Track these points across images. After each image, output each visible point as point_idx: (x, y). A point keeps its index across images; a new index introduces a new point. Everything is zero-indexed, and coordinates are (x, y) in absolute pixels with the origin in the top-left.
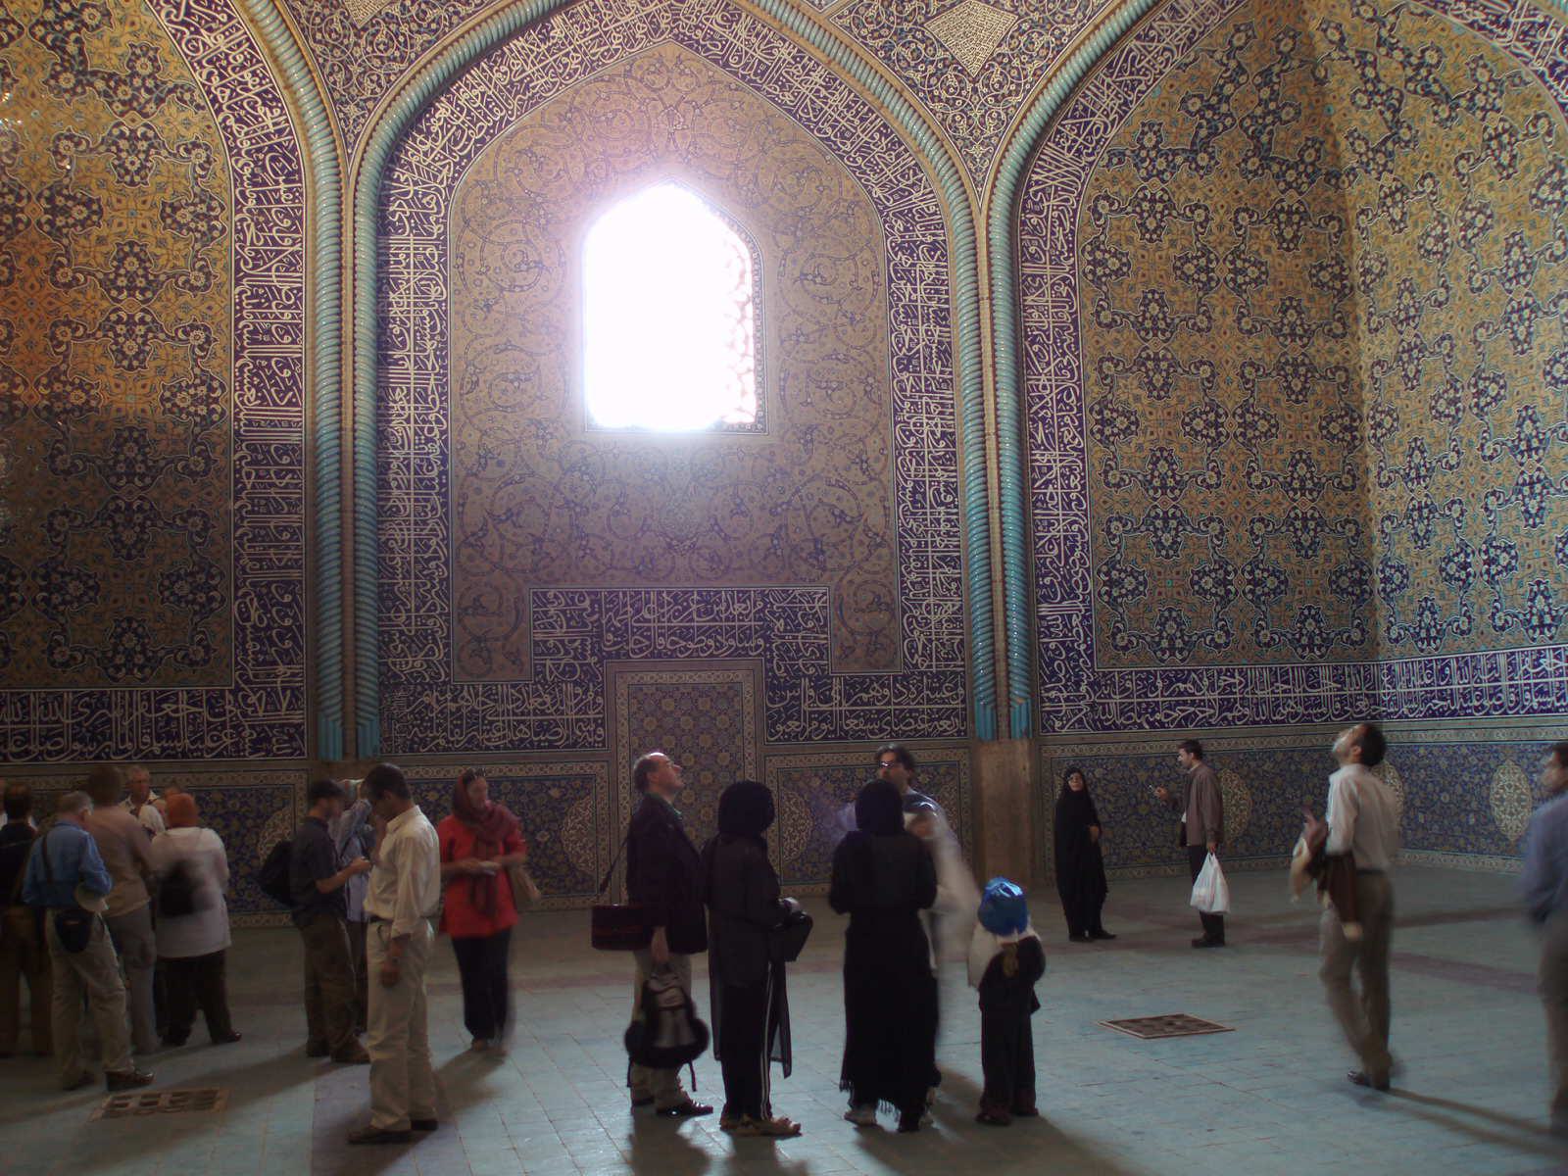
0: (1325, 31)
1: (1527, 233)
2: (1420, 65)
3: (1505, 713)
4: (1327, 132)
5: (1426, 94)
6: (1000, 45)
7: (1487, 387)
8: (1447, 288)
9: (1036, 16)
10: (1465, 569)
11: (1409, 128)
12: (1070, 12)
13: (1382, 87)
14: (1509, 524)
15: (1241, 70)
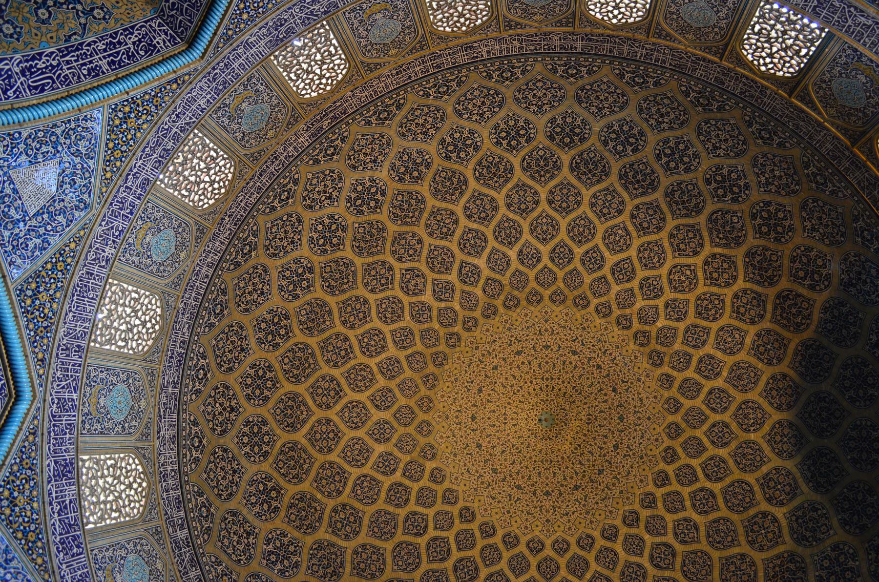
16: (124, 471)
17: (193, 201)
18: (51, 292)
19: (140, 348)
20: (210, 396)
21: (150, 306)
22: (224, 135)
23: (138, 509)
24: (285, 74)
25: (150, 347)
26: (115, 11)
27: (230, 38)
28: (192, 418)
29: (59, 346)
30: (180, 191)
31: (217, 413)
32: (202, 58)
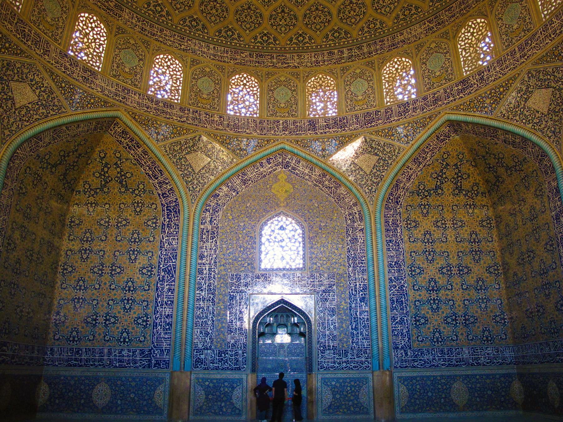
0: (100, 152)
1: (141, 231)
2: (124, 175)
3: (104, 367)
4: (79, 178)
5: (120, 183)
6: (29, 104)
7: (115, 269)
8: (106, 237)
9: (44, 102)
10: (95, 320)
11: (108, 189)
12: (55, 108)
13: (107, 175)
14: (117, 310)
15: (77, 151)
16: (314, 90)
17: (180, 75)
18: (239, 142)
19: (256, 84)
20: (276, 29)
21: (236, 84)
22: (145, 73)
23: (332, 81)
24: (103, 55)
25: (255, 78)
26: (114, 149)
27: (105, 102)
28: (289, 42)
29: (261, 134)
30: (178, 86)
31: (285, 23)
32: (119, 110)
